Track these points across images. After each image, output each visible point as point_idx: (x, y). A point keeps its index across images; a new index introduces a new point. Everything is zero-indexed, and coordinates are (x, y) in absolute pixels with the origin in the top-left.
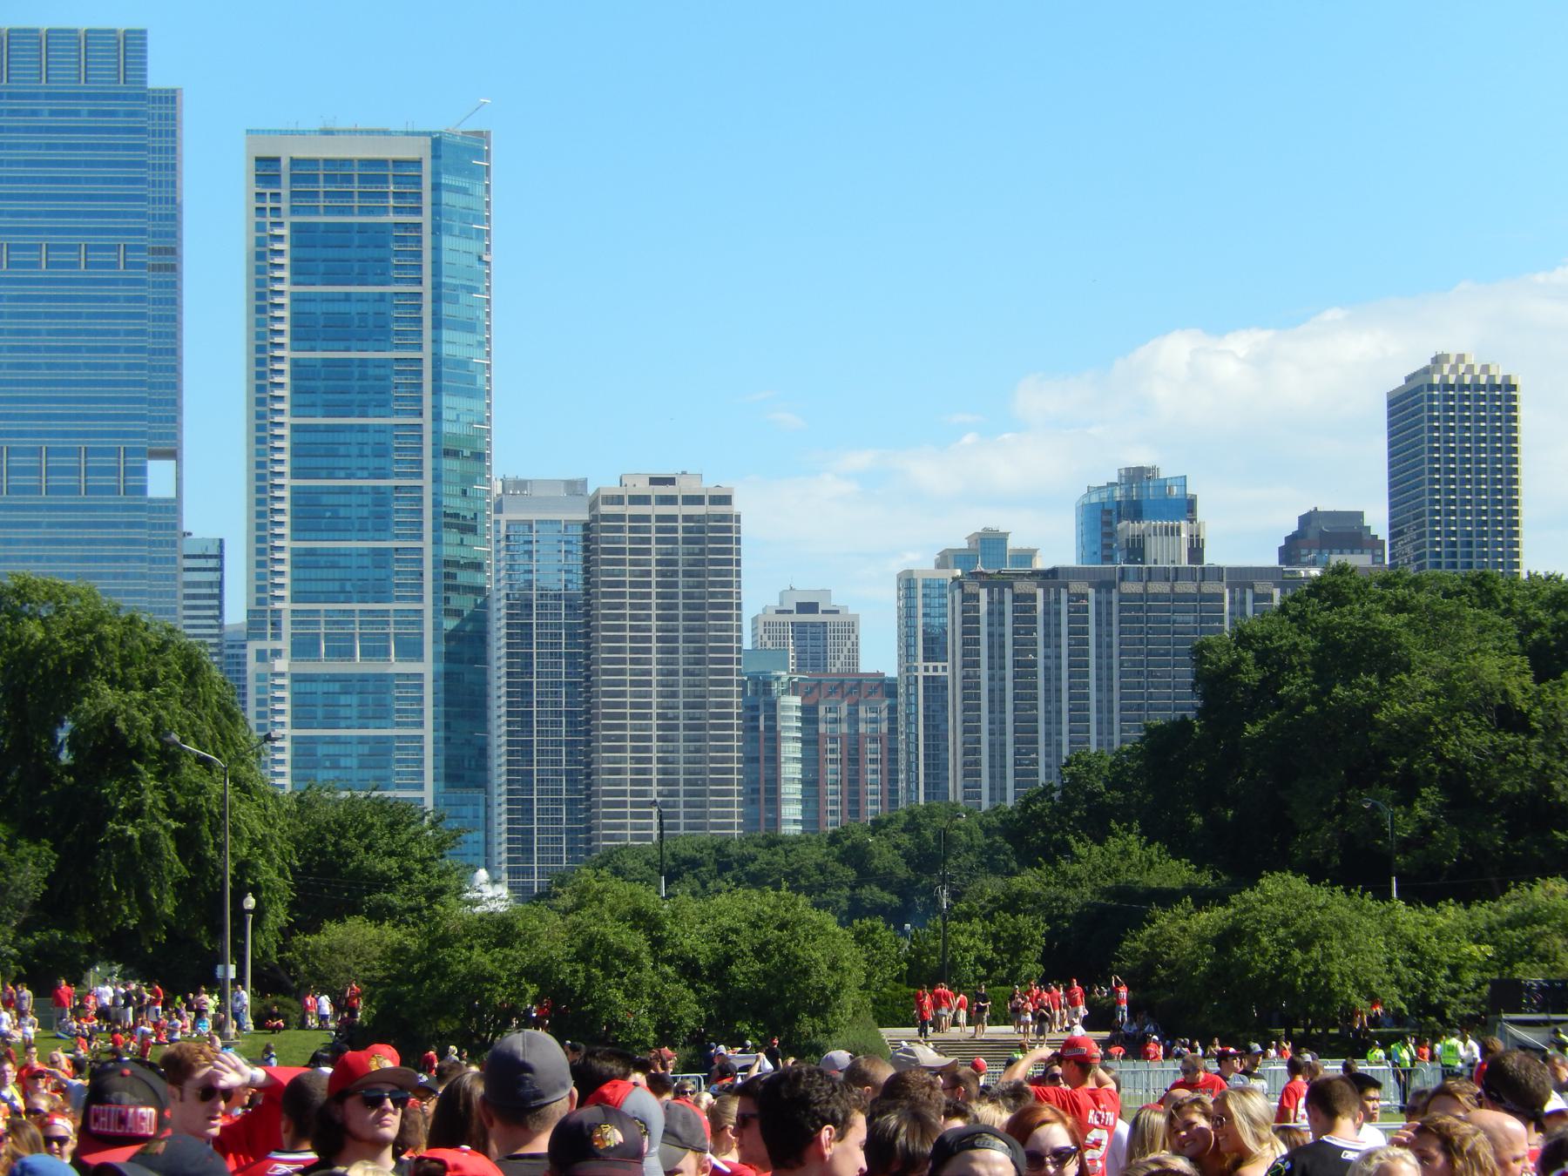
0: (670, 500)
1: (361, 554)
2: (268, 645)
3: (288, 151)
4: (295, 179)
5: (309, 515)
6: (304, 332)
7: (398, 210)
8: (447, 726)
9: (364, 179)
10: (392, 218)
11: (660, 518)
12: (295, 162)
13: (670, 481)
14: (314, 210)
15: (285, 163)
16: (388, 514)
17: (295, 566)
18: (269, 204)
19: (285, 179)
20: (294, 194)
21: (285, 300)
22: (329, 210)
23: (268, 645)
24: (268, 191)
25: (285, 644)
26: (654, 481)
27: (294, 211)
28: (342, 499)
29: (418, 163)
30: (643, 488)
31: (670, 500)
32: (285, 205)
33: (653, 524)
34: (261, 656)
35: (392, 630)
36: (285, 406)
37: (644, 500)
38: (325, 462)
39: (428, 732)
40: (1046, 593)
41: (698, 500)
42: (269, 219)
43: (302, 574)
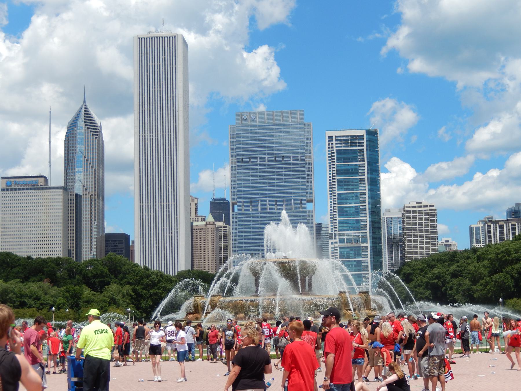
0: (421, 207)
1: (353, 220)
2: (334, 241)
3: (334, 134)
4: (336, 140)
5: (342, 212)
6: (340, 173)
7: (359, 146)
8: (373, 258)
11: (419, 211)
12: (336, 137)
13: (421, 203)
14: (341, 147)
15: (334, 138)
16: (359, 212)
17: (339, 223)
20: (336, 144)
21: (335, 166)
22: (344, 147)
23: (334, 241)
25: (337, 240)
26: (417, 203)
27: (336, 147)
28: (349, 209)
29: (363, 136)
30: (415, 204)
31: (421, 207)
32: (334, 145)
33: (417, 212)
34: (332, 243)
35: (360, 236)
36: (336, 189)
37: (415, 207)
38: (345, 201)
39: (369, 259)
40: (506, 225)
41: (427, 206)
42: (331, 149)
43: (339, 156)
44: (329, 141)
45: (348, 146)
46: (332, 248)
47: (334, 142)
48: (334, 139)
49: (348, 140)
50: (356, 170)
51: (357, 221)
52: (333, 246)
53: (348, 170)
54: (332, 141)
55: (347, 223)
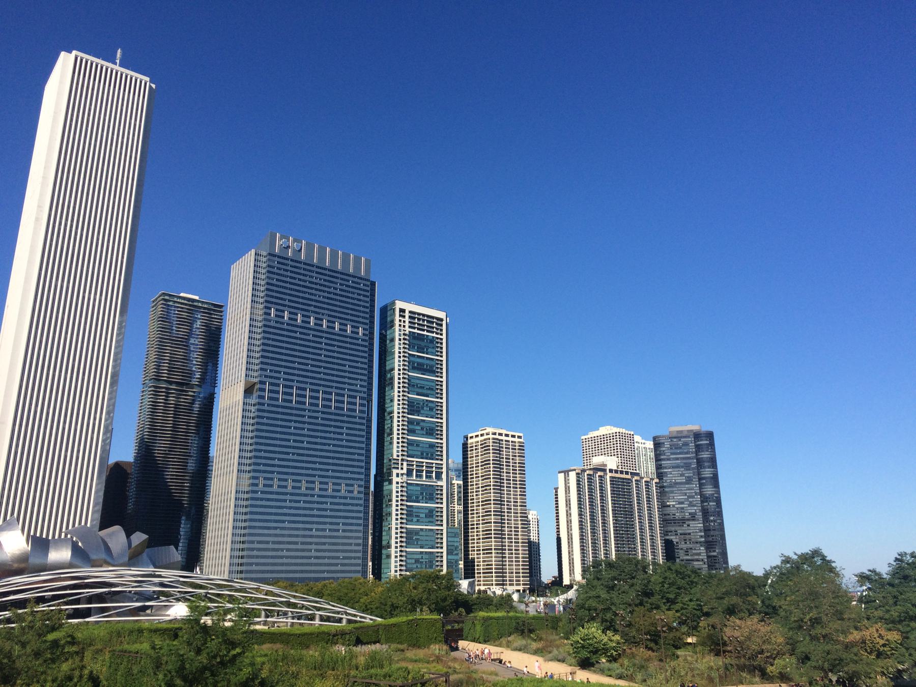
2: (400, 471)
3: (409, 307)
4: (410, 317)
7: (437, 333)
9: (428, 321)
10: (434, 335)
12: (410, 312)
14: (414, 328)
15: (407, 312)
18: (402, 324)
19: (407, 317)
23: (400, 471)
25: (405, 471)
27: (410, 327)
29: (442, 320)
32: (407, 324)
34: (398, 475)
44: (400, 316)
45: (423, 330)
46: (397, 483)
48: (407, 314)
50: (432, 366)
51: (432, 446)
52: (399, 479)
53: (422, 365)
54: (404, 317)
55: (418, 445)
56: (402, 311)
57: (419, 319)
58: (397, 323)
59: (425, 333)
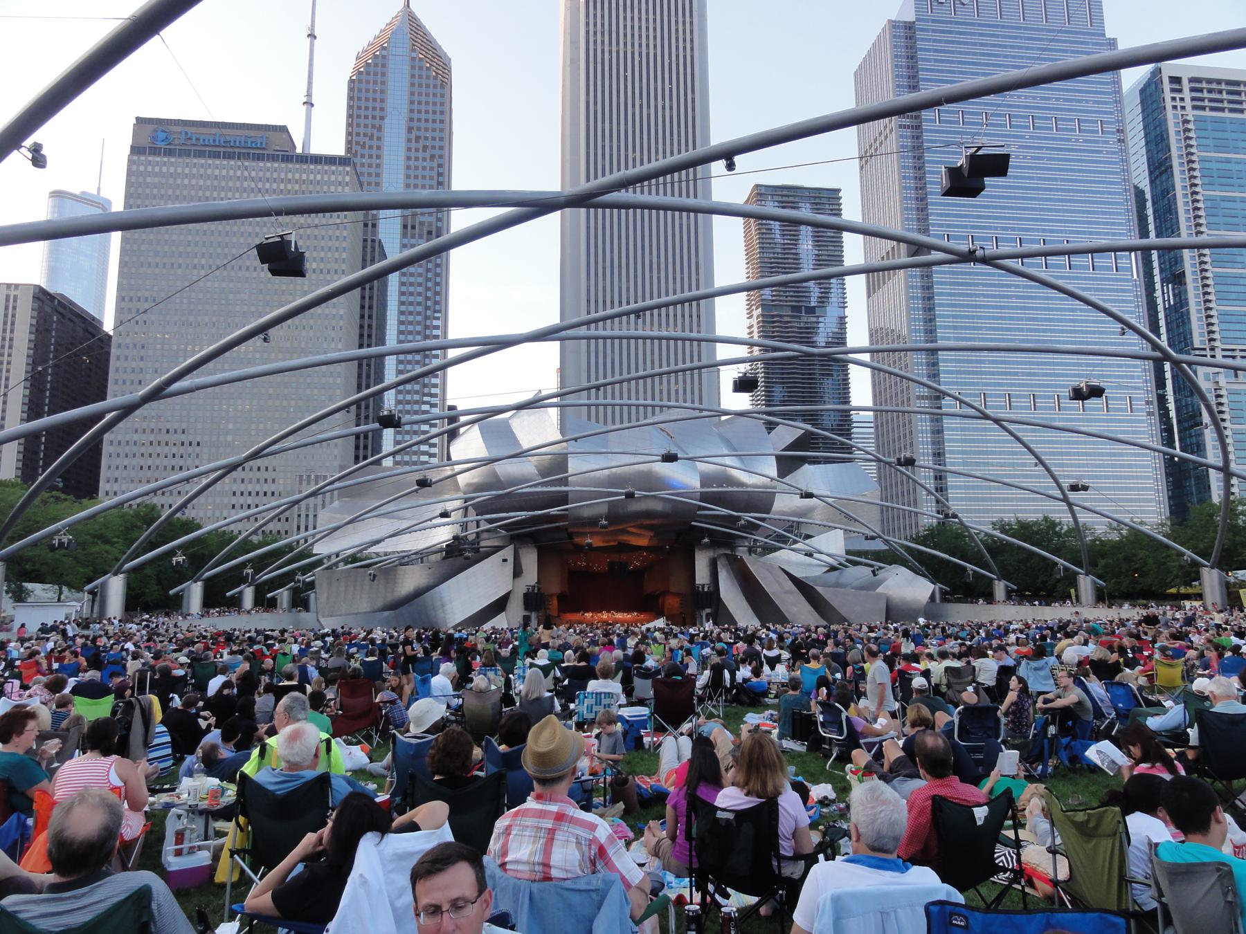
4: (1192, 90)
12: (1192, 80)
14: (1203, 108)
18: (1178, 104)
24: (1178, 96)
32: (1188, 103)
44: (1173, 90)
47: (1187, 94)
48: (1186, 86)
49: (1220, 92)
54: (1180, 91)
56: (1176, 80)
57: (1210, 91)
58: (1169, 104)
59: (1227, 114)
